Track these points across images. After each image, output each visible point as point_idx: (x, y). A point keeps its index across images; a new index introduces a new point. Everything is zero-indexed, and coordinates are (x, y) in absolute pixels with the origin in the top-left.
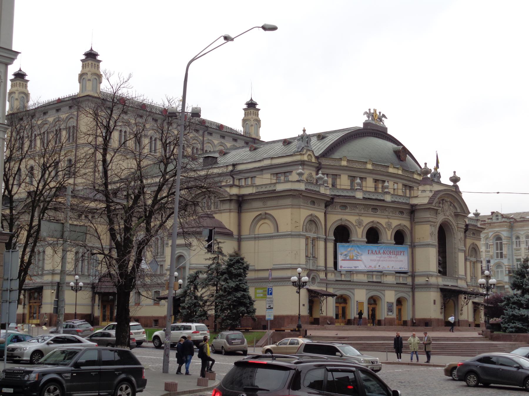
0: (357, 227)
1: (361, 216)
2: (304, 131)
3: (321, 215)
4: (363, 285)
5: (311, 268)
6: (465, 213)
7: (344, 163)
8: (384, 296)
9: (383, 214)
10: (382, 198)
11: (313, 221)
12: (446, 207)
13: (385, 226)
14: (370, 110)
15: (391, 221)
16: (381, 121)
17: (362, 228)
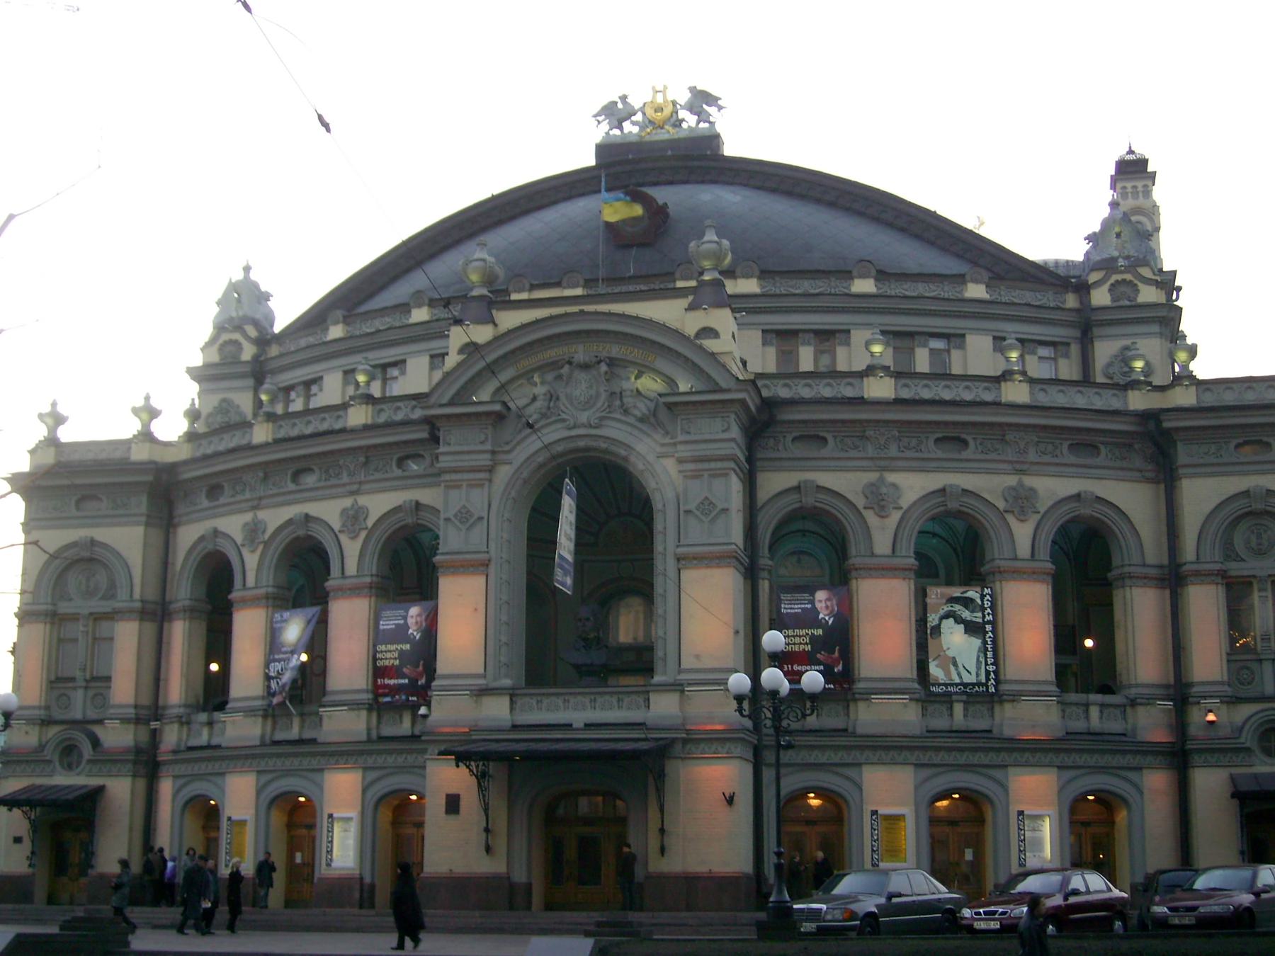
0: (245, 552)
1: (255, 508)
2: (247, 269)
3: (128, 540)
4: (247, 757)
5: (78, 715)
6: (722, 390)
7: (336, 332)
8: (321, 788)
9: (333, 481)
10: (338, 426)
11: (91, 560)
12: (582, 386)
13: (336, 526)
14: (624, 98)
15: (363, 500)
16: (702, 116)
17: (261, 547)
